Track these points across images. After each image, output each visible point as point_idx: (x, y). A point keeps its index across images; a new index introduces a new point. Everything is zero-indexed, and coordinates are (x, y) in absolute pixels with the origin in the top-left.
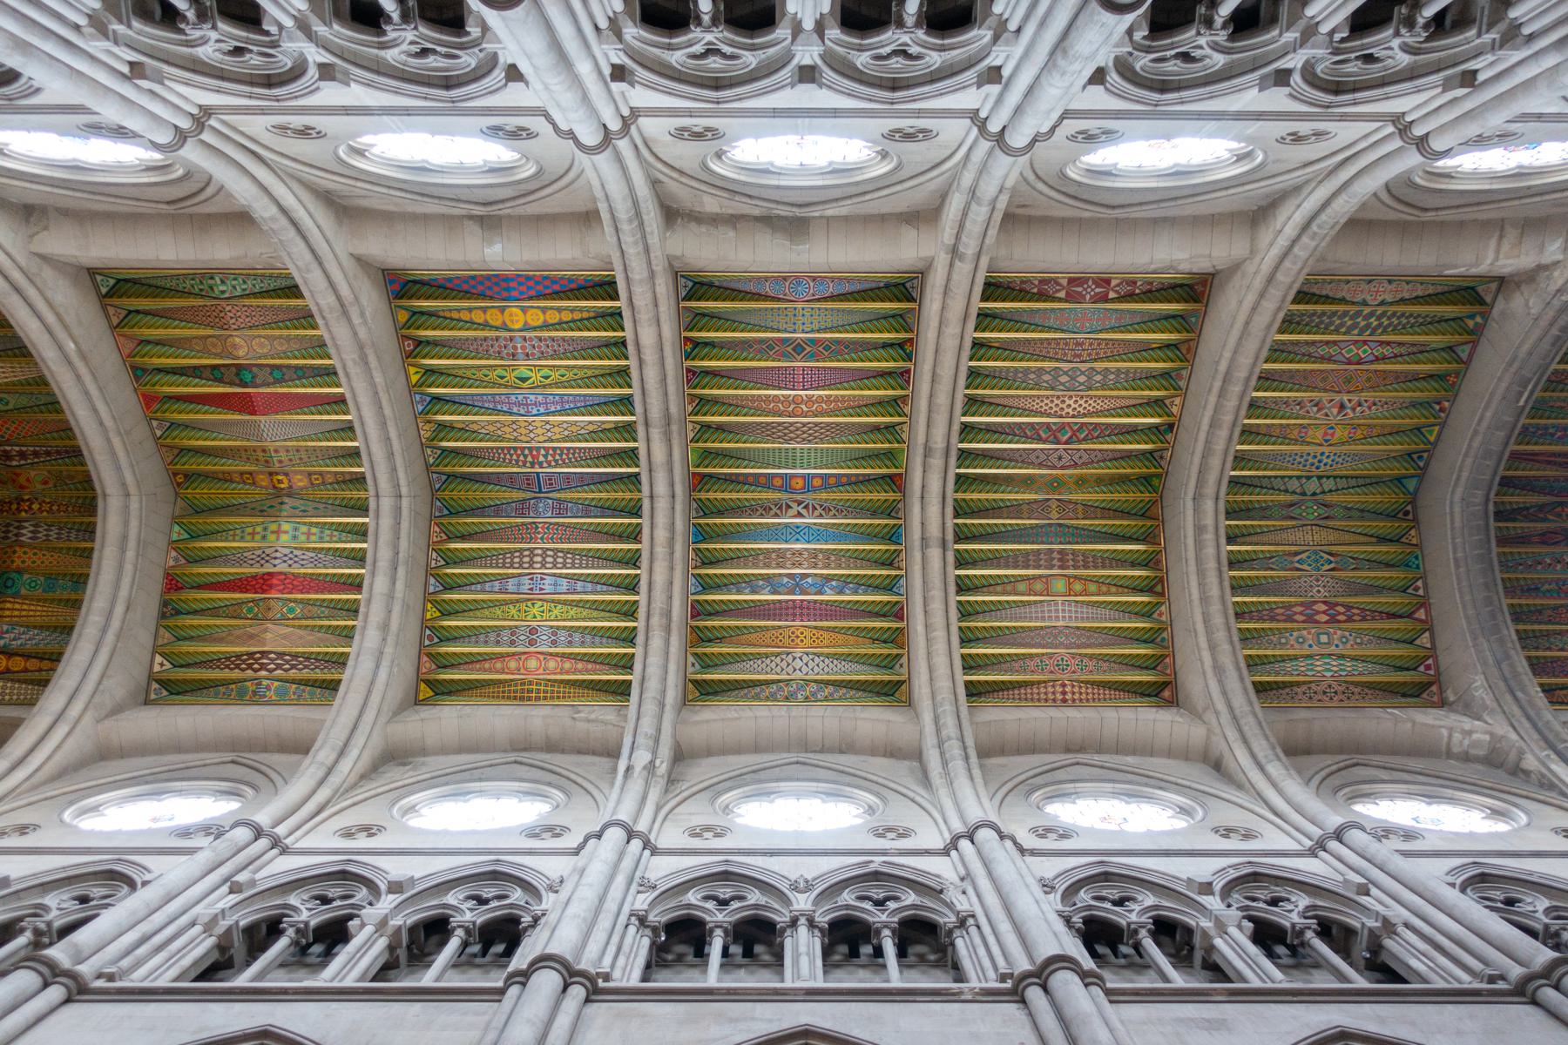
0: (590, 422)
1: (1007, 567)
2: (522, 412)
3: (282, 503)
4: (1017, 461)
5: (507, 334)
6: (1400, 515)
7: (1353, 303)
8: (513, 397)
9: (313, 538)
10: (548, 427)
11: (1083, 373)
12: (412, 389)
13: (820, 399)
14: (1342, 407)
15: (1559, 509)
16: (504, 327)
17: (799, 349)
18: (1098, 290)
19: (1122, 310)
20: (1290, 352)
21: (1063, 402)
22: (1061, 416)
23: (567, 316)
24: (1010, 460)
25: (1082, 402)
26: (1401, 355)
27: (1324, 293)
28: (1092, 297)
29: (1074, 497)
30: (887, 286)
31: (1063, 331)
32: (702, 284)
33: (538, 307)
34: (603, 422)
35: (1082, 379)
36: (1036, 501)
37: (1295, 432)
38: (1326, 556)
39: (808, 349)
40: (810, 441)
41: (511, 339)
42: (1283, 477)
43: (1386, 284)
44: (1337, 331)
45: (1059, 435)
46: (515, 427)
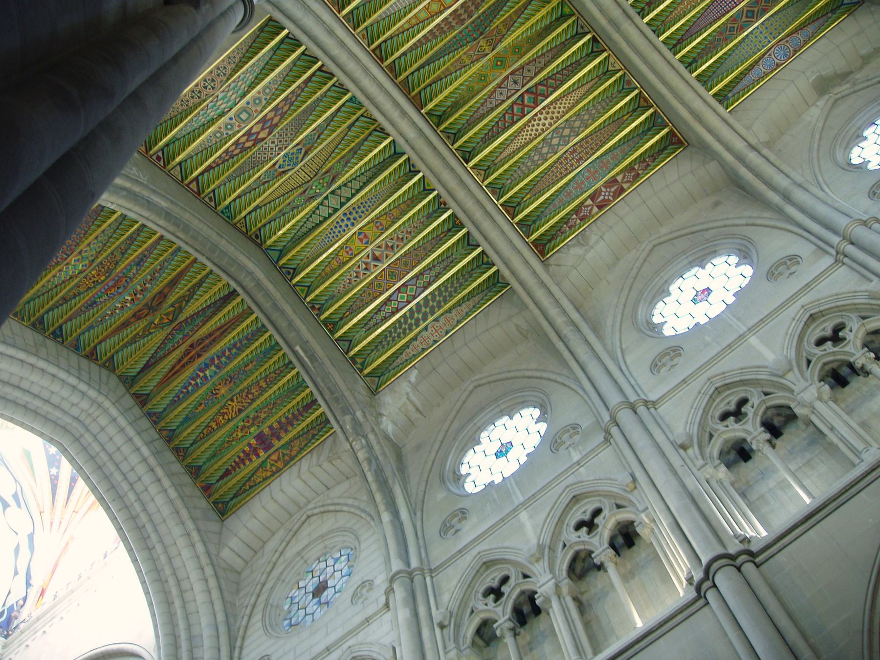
4: (539, 57)
11: (559, 145)
14: (376, 259)
15: (170, 318)
17: (750, 14)
18: (601, 198)
19: (574, 200)
20: (443, 261)
21: (552, 118)
22: (544, 108)
24: (543, 54)
25: (540, 128)
26: (376, 313)
29: (479, 65)
31: (597, 158)
35: (555, 141)
36: (500, 41)
37: (384, 222)
38: (287, 168)
39: (744, 19)
43: (436, 339)
45: (533, 96)
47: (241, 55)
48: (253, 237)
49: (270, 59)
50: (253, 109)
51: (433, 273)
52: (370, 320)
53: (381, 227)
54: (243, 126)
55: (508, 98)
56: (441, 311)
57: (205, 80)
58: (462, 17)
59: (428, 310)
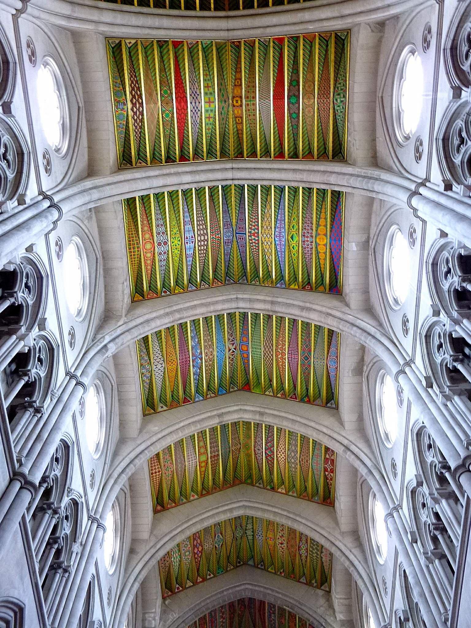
0: (272, 261)
1: (210, 435)
2: (276, 233)
3: (225, 101)
5: (314, 235)
6: (239, 560)
8: (283, 230)
9: (207, 120)
10: (269, 243)
16: (317, 234)
22: (277, 452)
23: (322, 262)
29: (242, 452)
30: (333, 393)
31: (312, 456)
33: (326, 251)
34: (272, 267)
39: (306, 362)
41: (312, 236)
42: (253, 523)
46: (269, 228)
48: (238, 565)
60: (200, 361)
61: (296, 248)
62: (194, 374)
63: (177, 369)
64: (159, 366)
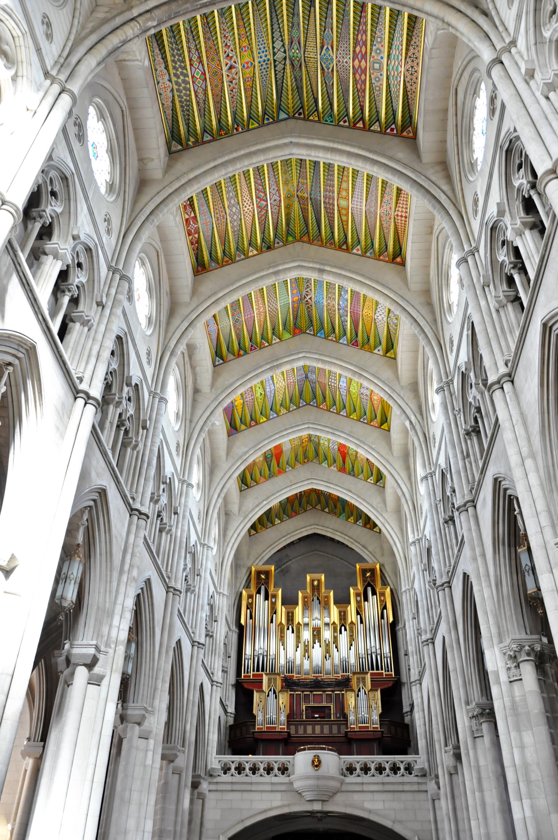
5: (246, 403)
7: (173, 96)
11: (231, 211)
12: (268, 419)
13: (258, 305)
18: (192, 223)
22: (254, 210)
25: (245, 204)
27: (171, 112)
28: (196, 224)
32: (216, 354)
38: (324, 51)
40: (277, 302)
44: (190, 95)
47: (409, 97)
49: (392, 106)
50: (375, 74)
51: (201, 101)
52: (193, 37)
53: (247, 80)
54: (372, 59)
55: (270, 192)
56: (176, 97)
57: (416, 71)
58: (327, 200)
59: (181, 88)
60: (341, 303)
61: (257, 389)
62: (347, 291)
63: (363, 307)
64: (380, 318)
